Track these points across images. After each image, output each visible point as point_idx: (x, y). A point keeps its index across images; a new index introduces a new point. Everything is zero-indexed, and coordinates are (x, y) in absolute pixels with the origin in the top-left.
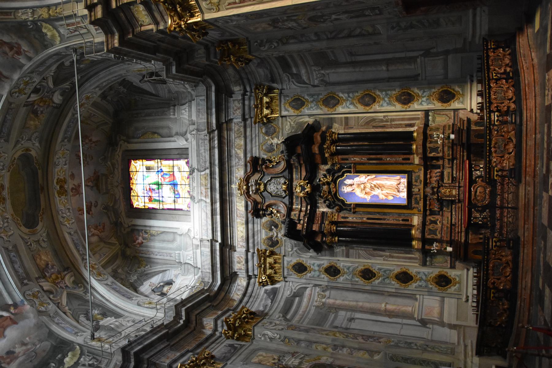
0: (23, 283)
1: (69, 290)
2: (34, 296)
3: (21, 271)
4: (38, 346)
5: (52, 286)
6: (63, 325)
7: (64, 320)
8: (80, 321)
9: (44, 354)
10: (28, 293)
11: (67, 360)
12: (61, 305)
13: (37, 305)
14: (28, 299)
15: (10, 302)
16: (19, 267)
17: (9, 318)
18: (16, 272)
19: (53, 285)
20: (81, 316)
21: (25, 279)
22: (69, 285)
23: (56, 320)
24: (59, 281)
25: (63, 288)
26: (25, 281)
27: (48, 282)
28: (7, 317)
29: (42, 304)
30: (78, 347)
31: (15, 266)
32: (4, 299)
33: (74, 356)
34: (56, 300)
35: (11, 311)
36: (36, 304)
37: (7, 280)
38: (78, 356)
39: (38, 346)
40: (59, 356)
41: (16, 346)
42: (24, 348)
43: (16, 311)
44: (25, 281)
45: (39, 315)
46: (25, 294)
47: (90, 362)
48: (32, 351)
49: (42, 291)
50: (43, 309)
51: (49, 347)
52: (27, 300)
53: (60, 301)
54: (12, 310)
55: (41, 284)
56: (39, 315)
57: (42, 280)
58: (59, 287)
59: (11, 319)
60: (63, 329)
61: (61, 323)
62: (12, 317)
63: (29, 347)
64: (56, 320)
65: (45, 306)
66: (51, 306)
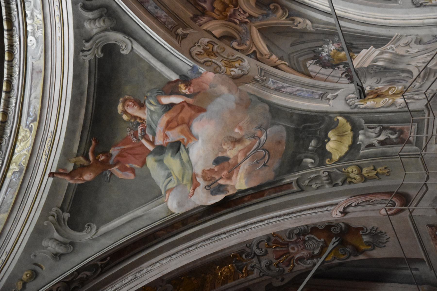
0: (178, 35)
1: (258, 23)
2: (210, 53)
3: (162, 14)
4: (263, 138)
5: (226, 26)
6: (289, 90)
7: (284, 80)
8: (312, 74)
9: (282, 148)
10: (196, 50)
11: (330, 146)
12: (261, 54)
13: (223, 68)
14: (202, 61)
15: (174, 77)
16: (156, 8)
17: (185, 104)
18: (156, 18)
19: (223, 22)
20: (308, 65)
22: (252, 13)
23: (270, 83)
24: (232, 10)
25: (246, 23)
27: (214, 19)
28: (182, 105)
29: (229, 64)
30: (340, 118)
31: (149, 8)
32: (160, 74)
33: (341, 135)
34: (248, 49)
35: (184, 91)
36: (220, 67)
37: (149, 39)
38: (350, 134)
39: (263, 138)
40: (313, 143)
41: (225, 147)
42: (239, 147)
43: (192, 89)
45: (238, 85)
46: (193, 54)
47: (382, 138)
48: (257, 148)
49: (216, 41)
50: (236, 72)
51: (284, 134)
52: (202, 64)
53: (254, 49)
54: (183, 89)
56: (238, 85)
57: (204, 19)
58: (238, 22)
59: (189, 105)
61: (283, 87)
62: (190, 101)
63: (248, 143)
64: (270, 83)
65: (237, 65)
66: (247, 61)
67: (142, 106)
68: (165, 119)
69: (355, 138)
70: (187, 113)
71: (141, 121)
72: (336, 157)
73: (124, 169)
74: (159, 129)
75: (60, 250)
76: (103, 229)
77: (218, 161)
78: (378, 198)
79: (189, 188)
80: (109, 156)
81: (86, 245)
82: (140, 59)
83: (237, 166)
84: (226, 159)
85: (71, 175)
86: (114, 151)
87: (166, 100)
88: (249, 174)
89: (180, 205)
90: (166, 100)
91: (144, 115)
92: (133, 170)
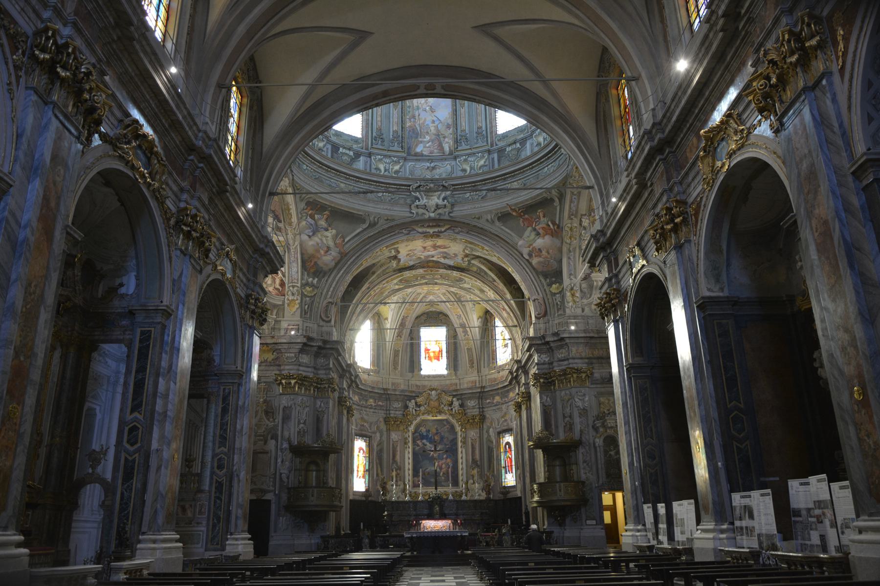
7: (574, 257)
11: (554, 286)
21: (572, 215)
26: (572, 217)
28: (551, 229)
32: (556, 217)
33: (558, 288)
38: (558, 291)
40: (554, 279)
44: (572, 217)
55: (583, 220)
60: (569, 263)
67: (544, 217)
69: (558, 293)
72: (551, 289)
73: (523, 222)
74: (541, 226)
75: (490, 220)
76: (503, 227)
77: (540, 249)
78: (543, 307)
79: (527, 245)
82: (556, 209)
83: (540, 256)
84: (541, 252)
85: (511, 209)
86: (526, 216)
87: (550, 223)
88: (539, 263)
89: (520, 246)
90: (550, 223)
91: (542, 219)
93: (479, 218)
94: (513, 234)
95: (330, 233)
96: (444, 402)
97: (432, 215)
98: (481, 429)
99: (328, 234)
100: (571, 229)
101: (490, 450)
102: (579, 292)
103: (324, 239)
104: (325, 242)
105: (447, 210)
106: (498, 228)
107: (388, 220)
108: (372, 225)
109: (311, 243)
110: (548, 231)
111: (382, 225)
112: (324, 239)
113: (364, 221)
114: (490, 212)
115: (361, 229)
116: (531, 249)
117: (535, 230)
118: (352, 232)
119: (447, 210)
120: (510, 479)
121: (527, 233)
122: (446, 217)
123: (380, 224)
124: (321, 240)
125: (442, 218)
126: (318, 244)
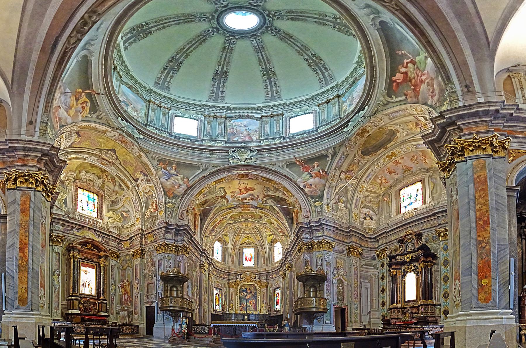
68: (317, 172)
70: (319, 176)
71: (314, 167)
73: (303, 169)
74: (314, 172)
75: (281, 166)
76: (289, 171)
80: (304, 165)
81: (284, 170)
85: (296, 160)
86: (306, 165)
87: (321, 171)
90: (321, 171)
92: (303, 170)
93: (274, 165)
94: (295, 175)
95: (180, 177)
96: (252, 277)
97: (243, 163)
98: (267, 288)
99: (177, 177)
100: (334, 176)
101: (270, 296)
102: (331, 207)
103: (176, 180)
104: (177, 182)
105: (253, 161)
106: (286, 171)
107: (214, 166)
108: (205, 170)
109: (168, 183)
110: (318, 175)
111: (211, 170)
112: (176, 180)
113: (199, 168)
114: (282, 161)
115: (198, 173)
116: (305, 184)
117: (310, 174)
118: (193, 175)
119: (253, 161)
120: (278, 308)
121: (304, 175)
122: (253, 164)
123: (209, 168)
124: (175, 181)
125: (249, 164)
126: (173, 183)
